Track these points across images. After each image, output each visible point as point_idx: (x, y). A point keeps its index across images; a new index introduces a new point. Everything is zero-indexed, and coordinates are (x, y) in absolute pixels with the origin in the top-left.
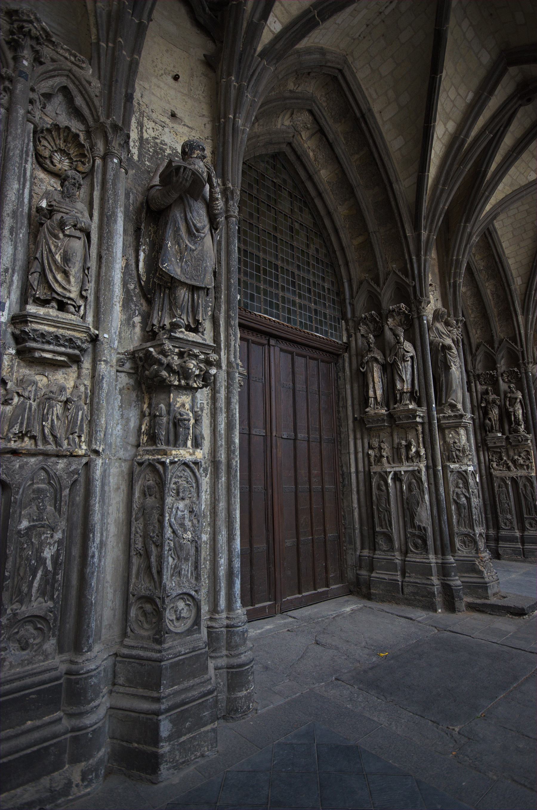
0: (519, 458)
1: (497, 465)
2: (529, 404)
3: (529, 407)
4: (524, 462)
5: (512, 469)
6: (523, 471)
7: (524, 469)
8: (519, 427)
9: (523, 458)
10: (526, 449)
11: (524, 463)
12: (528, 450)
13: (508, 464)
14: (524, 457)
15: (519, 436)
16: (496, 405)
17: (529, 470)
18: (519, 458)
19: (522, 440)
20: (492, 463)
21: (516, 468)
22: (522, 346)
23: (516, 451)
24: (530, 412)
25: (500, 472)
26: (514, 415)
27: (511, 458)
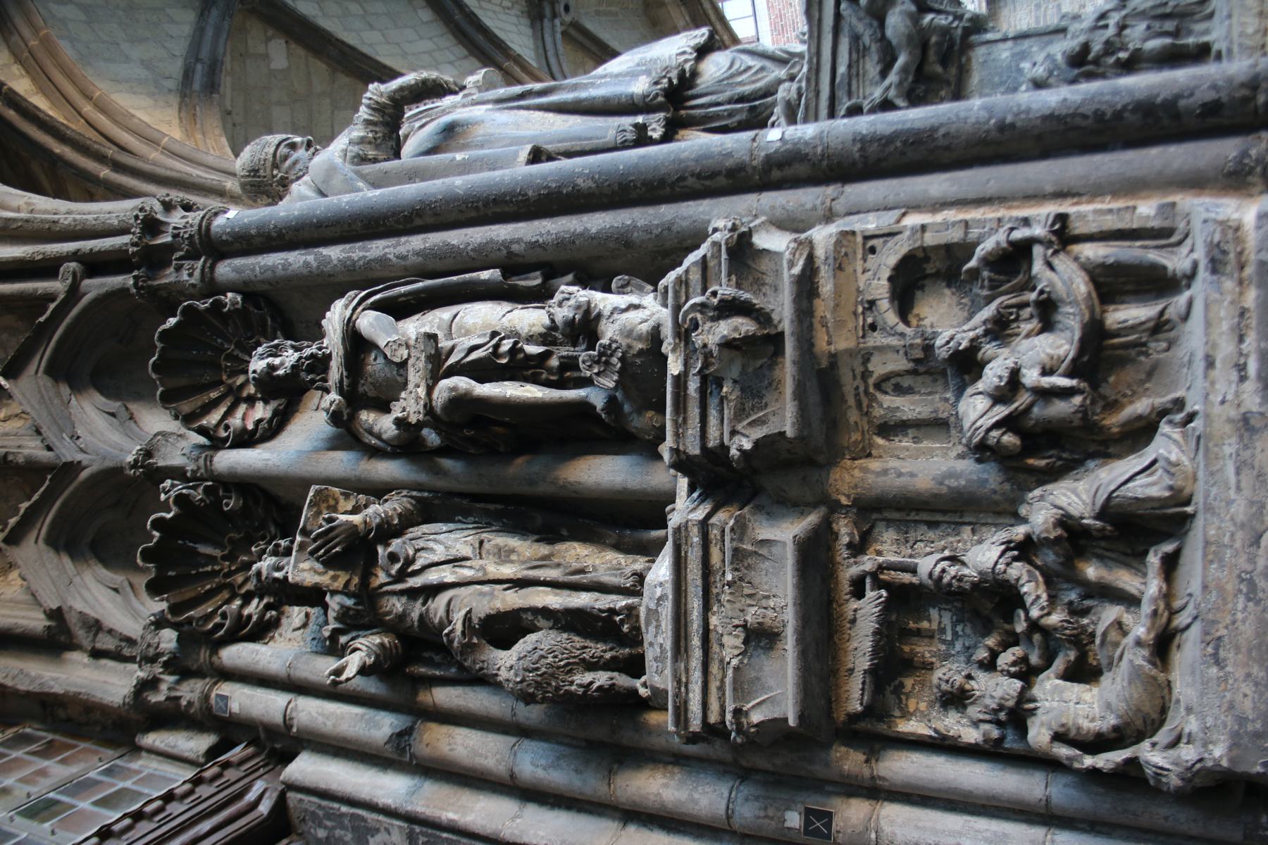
0: (994, 374)
1: (1083, 672)
2: (435, 239)
3: (455, 237)
4: (1047, 312)
5: (1151, 487)
6: (1193, 338)
7: (1159, 326)
8: (609, 332)
9: (1000, 329)
10: (880, 288)
11: (1072, 322)
12: (890, 256)
13: (1066, 522)
14: (988, 312)
15: (684, 334)
16: (388, 531)
17: (1176, 262)
18: (994, 374)
19: (729, 308)
20: (1039, 735)
21: (1142, 432)
22: (47, 268)
23: (908, 407)
24: (502, 232)
25: (1188, 652)
26: (483, 370)
27: (989, 477)
